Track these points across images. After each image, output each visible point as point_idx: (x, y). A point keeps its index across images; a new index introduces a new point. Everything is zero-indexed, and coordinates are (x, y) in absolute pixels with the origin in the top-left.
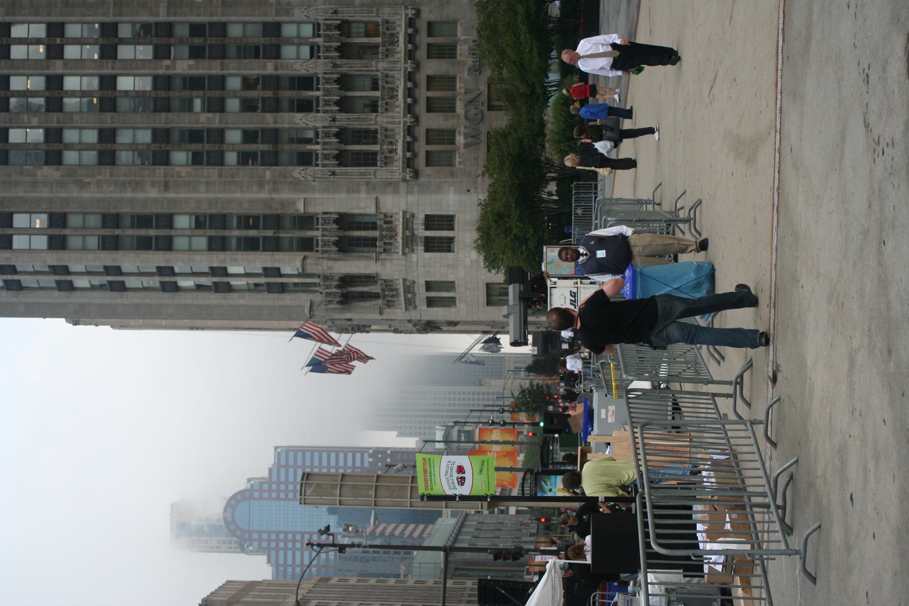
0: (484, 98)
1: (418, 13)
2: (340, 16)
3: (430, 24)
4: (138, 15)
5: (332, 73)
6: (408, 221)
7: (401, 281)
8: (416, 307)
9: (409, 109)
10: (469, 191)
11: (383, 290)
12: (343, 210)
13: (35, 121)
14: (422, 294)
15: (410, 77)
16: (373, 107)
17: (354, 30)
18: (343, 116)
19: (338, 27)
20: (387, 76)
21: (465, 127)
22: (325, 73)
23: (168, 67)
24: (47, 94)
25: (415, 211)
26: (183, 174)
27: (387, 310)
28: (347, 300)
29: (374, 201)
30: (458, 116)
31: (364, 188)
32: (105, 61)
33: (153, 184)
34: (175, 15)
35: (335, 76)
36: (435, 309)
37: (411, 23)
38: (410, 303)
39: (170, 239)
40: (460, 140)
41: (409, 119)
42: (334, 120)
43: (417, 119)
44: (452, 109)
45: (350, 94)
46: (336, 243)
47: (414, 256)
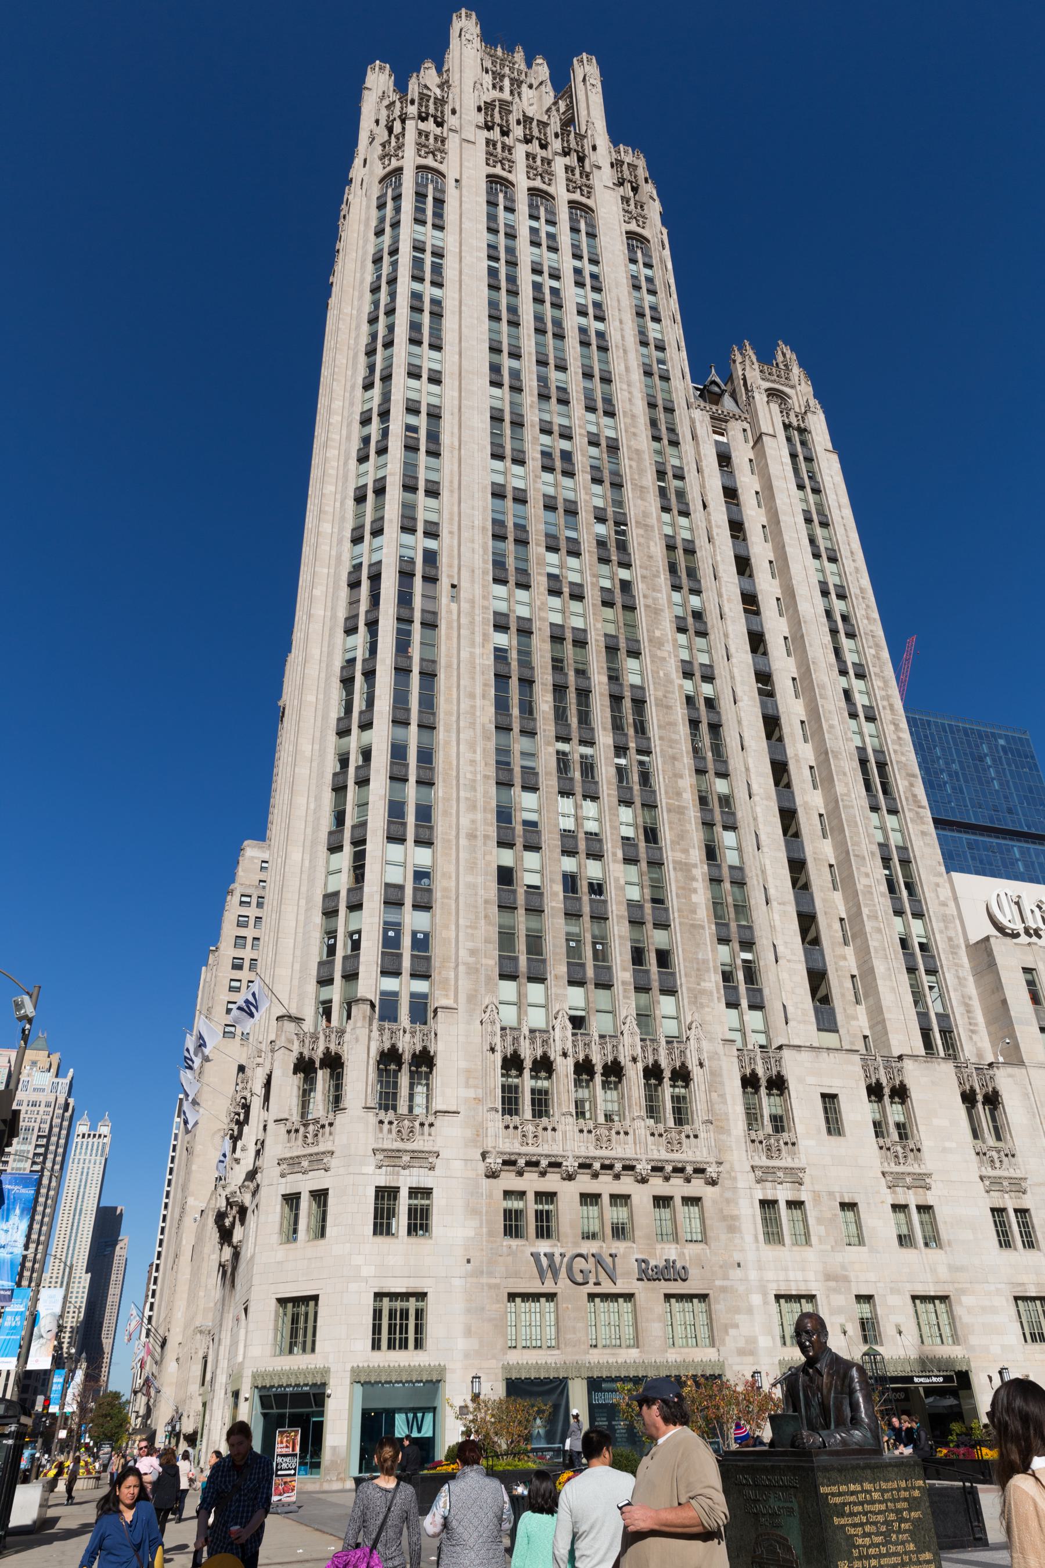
0: (607, 1287)
1: (713, 1183)
4: (671, 829)
6: (423, 1158)
7: (330, 1149)
8: (283, 1176)
10: (469, 1261)
11: (316, 1121)
12: (439, 1062)
14: (305, 1184)
21: (563, 1255)
23: (614, 854)
25: (438, 1172)
26: (488, 857)
27: (282, 1129)
28: (304, 1067)
29: (454, 1109)
30: (576, 1244)
31: (471, 1093)
33: (473, 822)
34: (675, 869)
35: (621, 1059)
36: (278, 1208)
38: (292, 1164)
39: (401, 840)
40: (543, 1247)
41: (570, 1165)
43: (570, 1177)
46: (393, 1049)
47: (370, 1169)
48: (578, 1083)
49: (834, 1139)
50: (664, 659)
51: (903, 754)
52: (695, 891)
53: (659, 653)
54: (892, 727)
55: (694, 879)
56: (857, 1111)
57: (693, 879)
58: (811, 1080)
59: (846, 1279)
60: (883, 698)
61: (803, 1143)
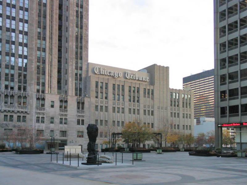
1: (28, 114)
2: (28, 97)
3: (25, 117)
5: (14, 94)
9: (5, 111)
13: (4, 24)
15: (13, 111)
16: (6, 103)
17: (24, 100)
18: (4, 96)
19: (25, 96)
20: (13, 106)
22: (14, 92)
23: (17, 57)
24: (11, 29)
32: (18, 43)
37: (26, 112)
42: (3, 93)
44: (5, 121)
45: (9, 98)
48: (5, 98)
49: (52, 108)
50: (33, 14)
51: (86, 37)
52: (33, 65)
53: (32, 12)
54: (85, 31)
55: (33, 63)
56: (57, 104)
57: (33, 63)
58: (50, 99)
59: (49, 128)
60: (85, 24)
61: (46, 109)
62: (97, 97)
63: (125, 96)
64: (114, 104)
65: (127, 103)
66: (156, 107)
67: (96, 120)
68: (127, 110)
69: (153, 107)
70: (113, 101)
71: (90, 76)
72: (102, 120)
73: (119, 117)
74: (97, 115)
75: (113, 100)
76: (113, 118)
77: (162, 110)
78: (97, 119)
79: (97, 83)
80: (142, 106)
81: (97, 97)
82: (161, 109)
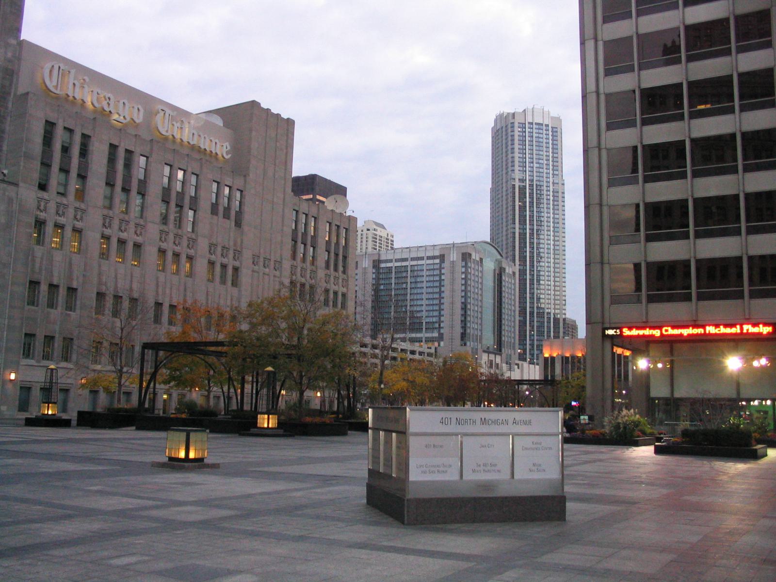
62: (43, 187)
63: (149, 199)
64: (107, 222)
65: (153, 230)
66: (247, 255)
67: (31, 282)
68: (151, 254)
69: (237, 254)
70: (106, 212)
71: (27, 94)
72: (57, 286)
73: (119, 274)
74: (38, 260)
75: (105, 207)
76: (100, 283)
77: (267, 270)
78: (35, 278)
79: (50, 126)
80: (203, 244)
81: (43, 187)
82: (262, 268)
